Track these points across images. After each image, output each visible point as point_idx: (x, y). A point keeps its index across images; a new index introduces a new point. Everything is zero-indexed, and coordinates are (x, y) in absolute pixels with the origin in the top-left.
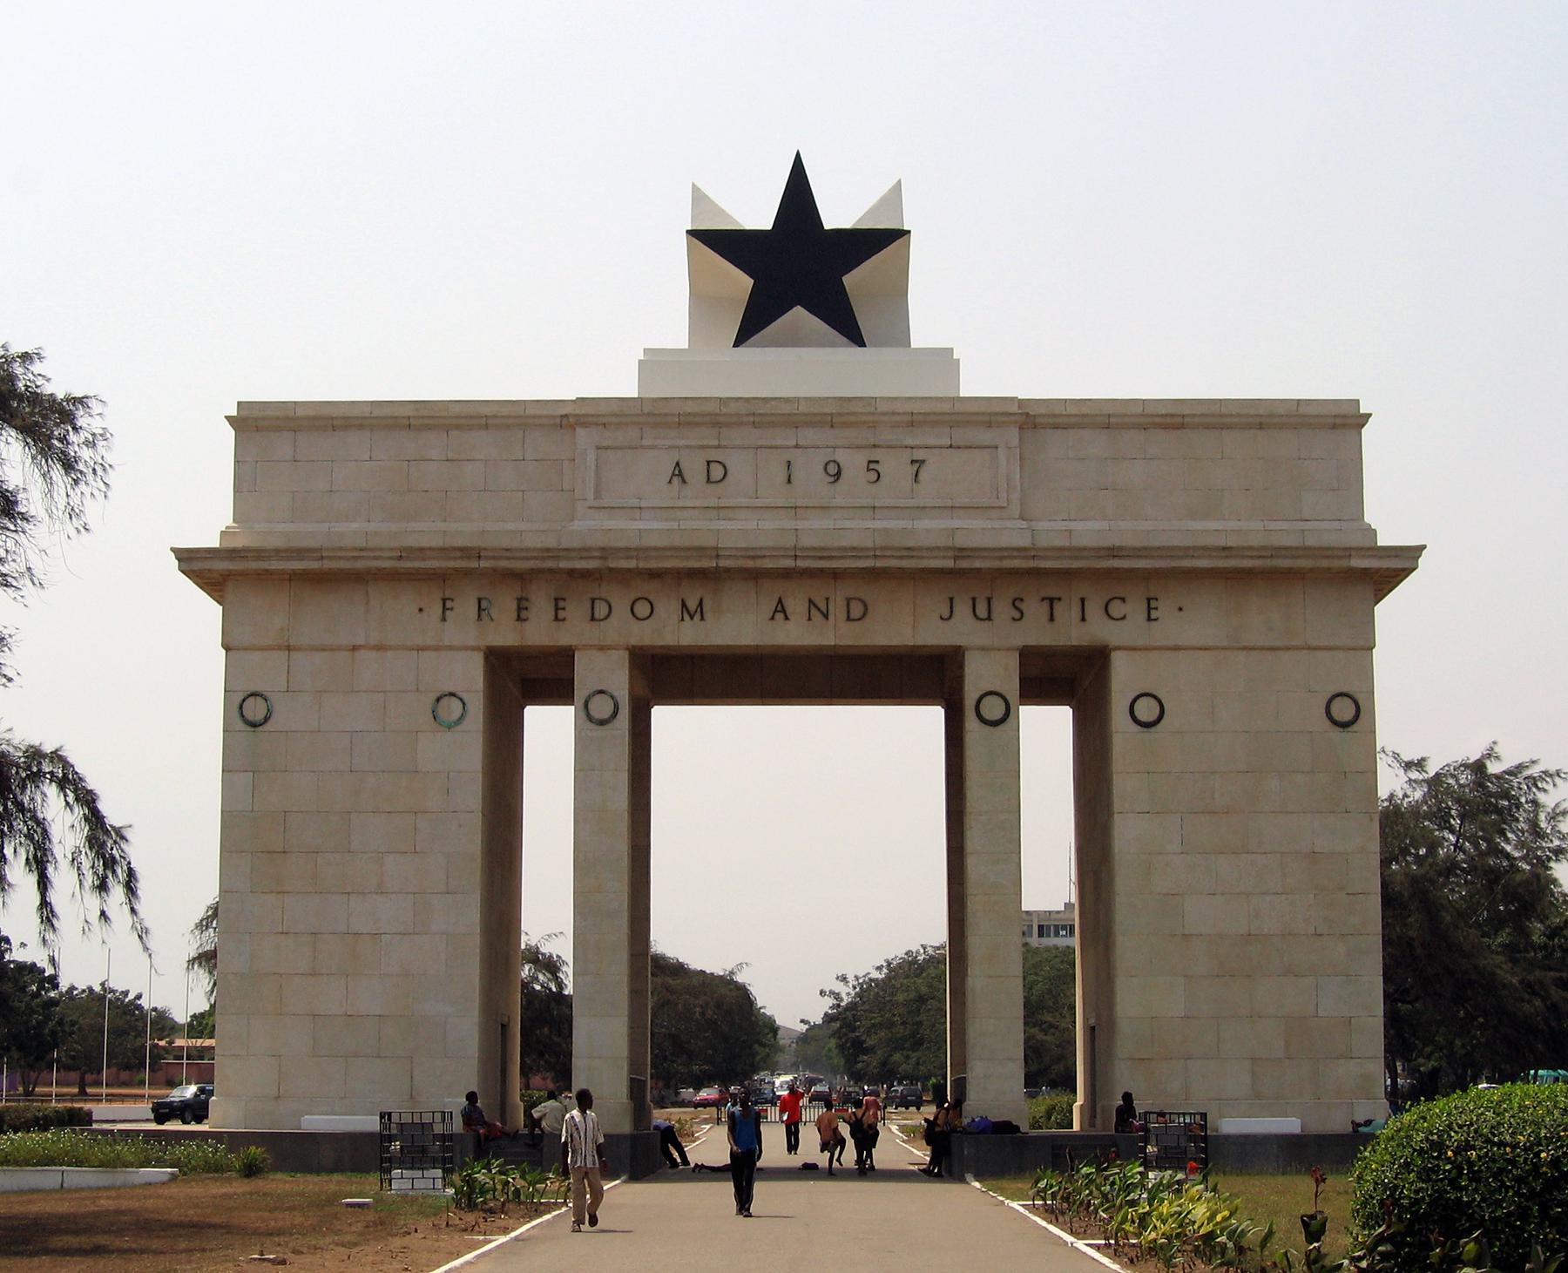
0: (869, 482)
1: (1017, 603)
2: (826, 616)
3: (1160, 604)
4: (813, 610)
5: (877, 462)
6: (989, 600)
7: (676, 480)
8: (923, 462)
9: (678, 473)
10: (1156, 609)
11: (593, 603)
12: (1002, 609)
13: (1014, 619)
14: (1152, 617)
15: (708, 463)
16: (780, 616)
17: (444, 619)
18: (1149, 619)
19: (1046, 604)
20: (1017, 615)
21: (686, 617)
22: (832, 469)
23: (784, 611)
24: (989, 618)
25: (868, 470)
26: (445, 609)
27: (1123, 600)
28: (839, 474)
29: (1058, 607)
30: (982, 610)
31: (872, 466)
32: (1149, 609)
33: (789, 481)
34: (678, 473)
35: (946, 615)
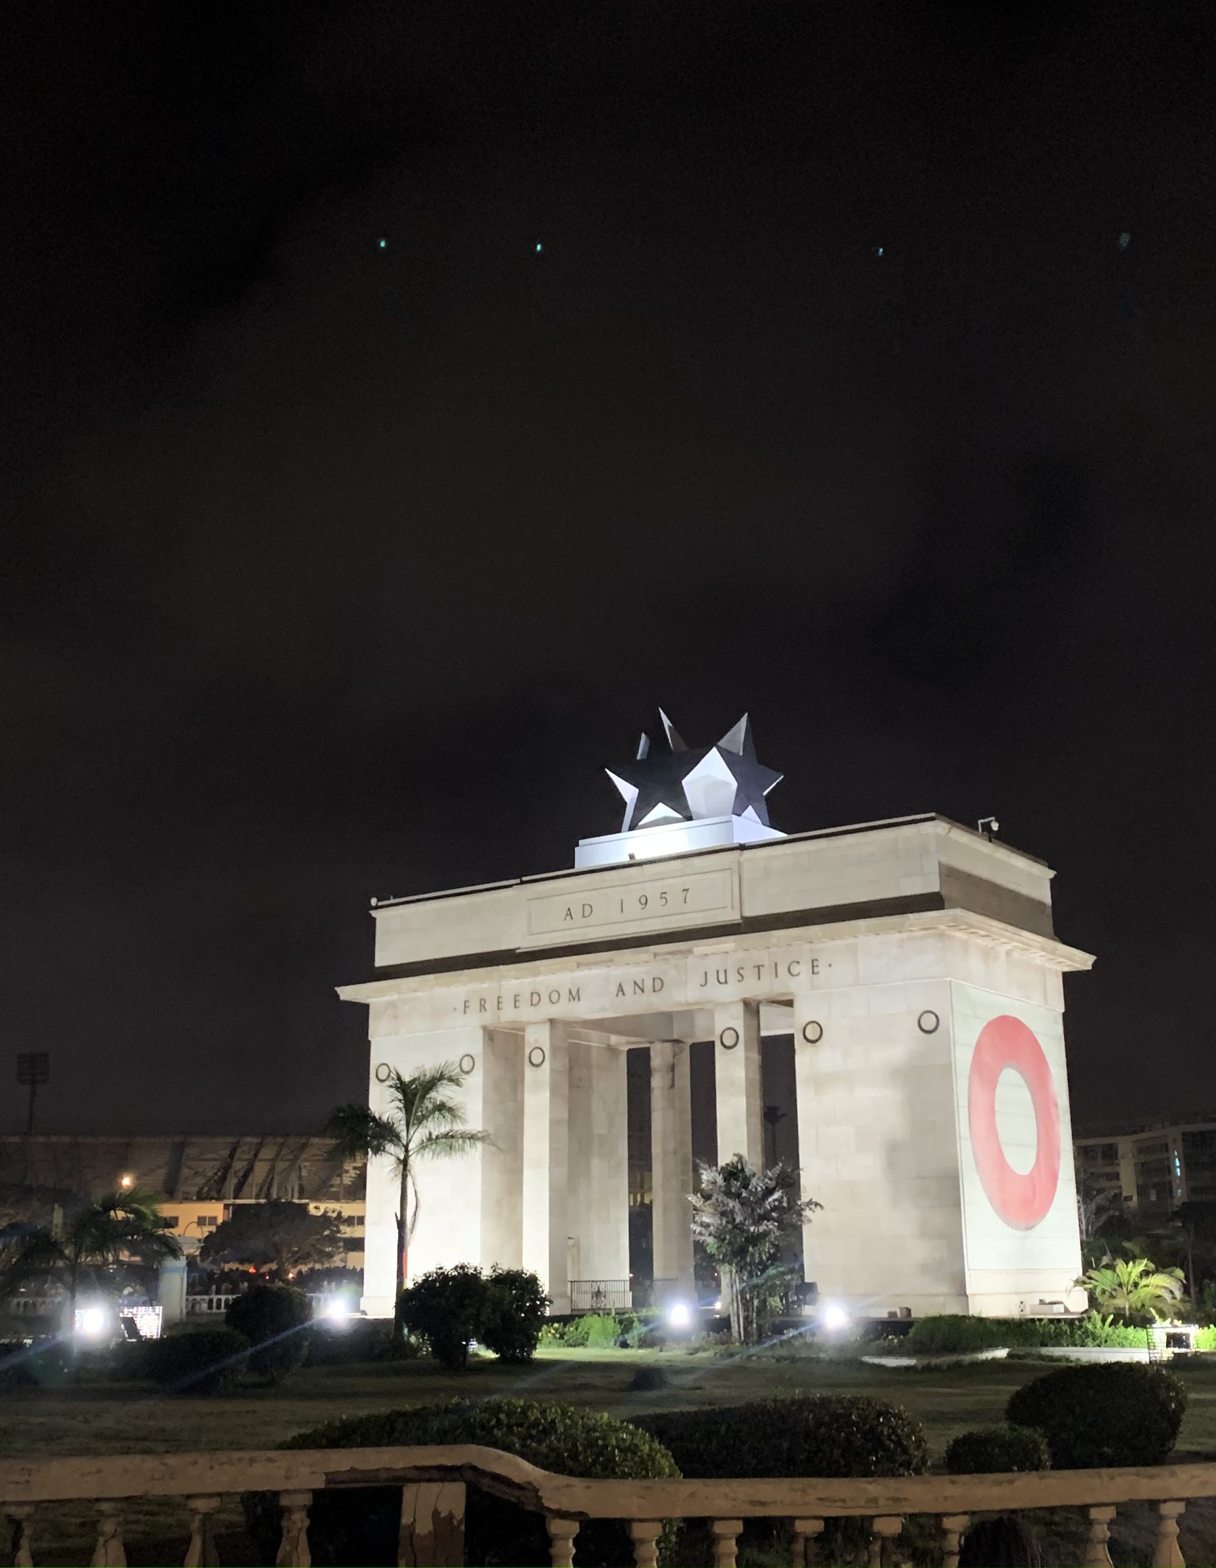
0: (664, 905)
1: (741, 972)
2: (643, 991)
3: (819, 963)
4: (636, 987)
5: (665, 893)
6: (726, 971)
7: (569, 917)
8: (687, 890)
9: (569, 913)
10: (817, 966)
11: (759, 970)
12: (733, 977)
13: (739, 981)
14: (815, 971)
15: (584, 905)
16: (620, 993)
17: (465, 1013)
18: (813, 973)
19: (757, 969)
20: (740, 978)
21: (571, 999)
22: (643, 901)
23: (622, 990)
24: (726, 982)
25: (661, 898)
26: (465, 1007)
27: (798, 962)
28: (646, 903)
29: (761, 968)
30: (722, 979)
31: (664, 895)
32: (813, 967)
33: (622, 911)
34: (569, 913)
35: (703, 984)
